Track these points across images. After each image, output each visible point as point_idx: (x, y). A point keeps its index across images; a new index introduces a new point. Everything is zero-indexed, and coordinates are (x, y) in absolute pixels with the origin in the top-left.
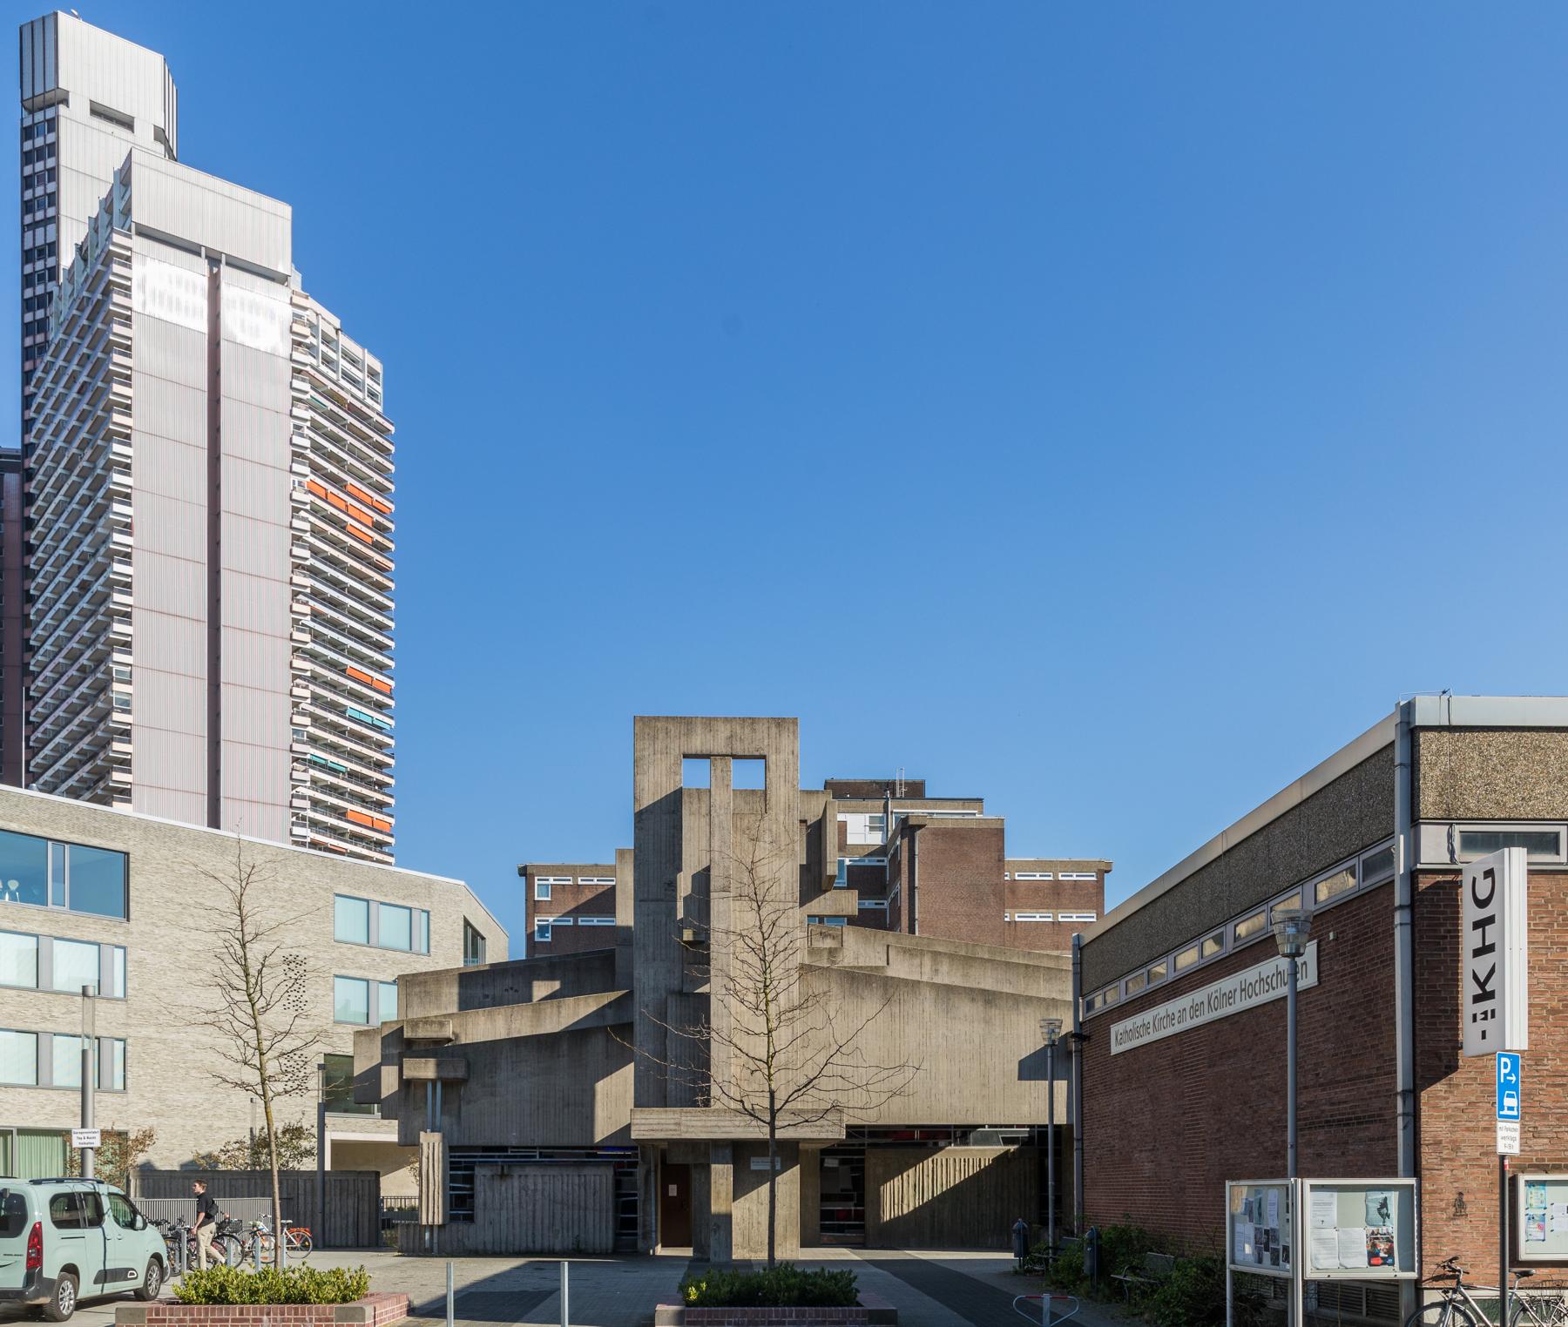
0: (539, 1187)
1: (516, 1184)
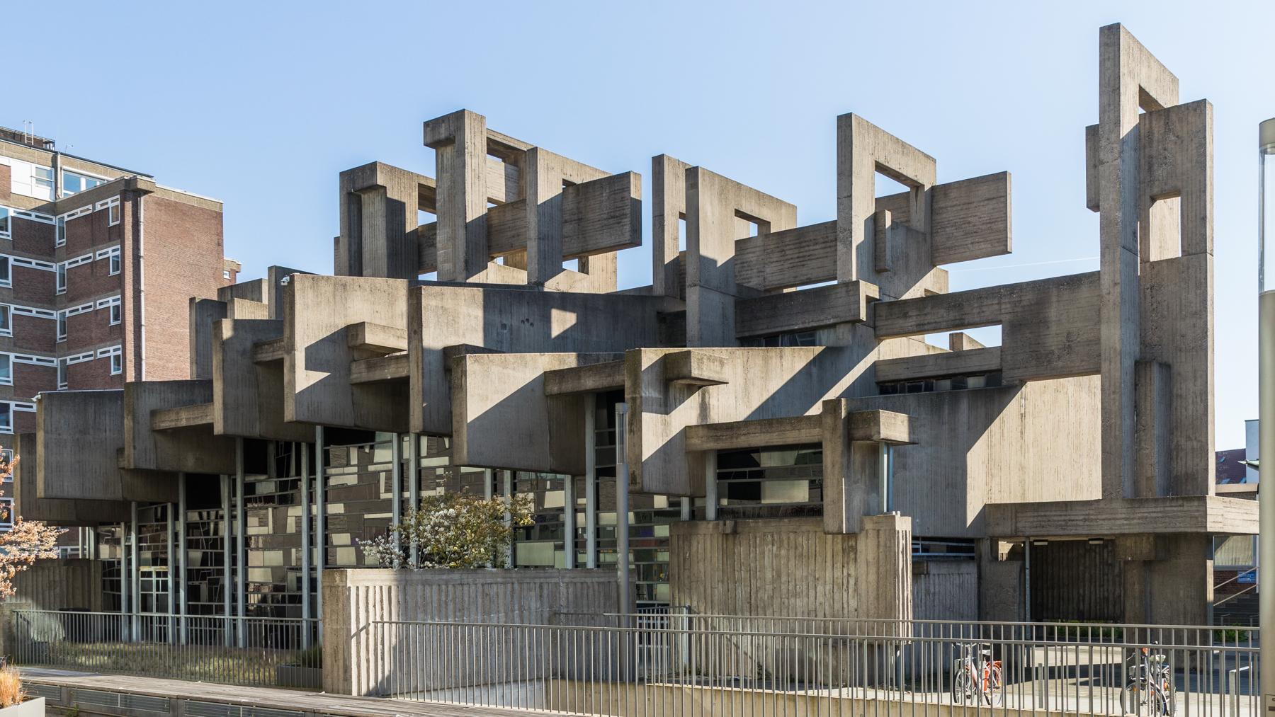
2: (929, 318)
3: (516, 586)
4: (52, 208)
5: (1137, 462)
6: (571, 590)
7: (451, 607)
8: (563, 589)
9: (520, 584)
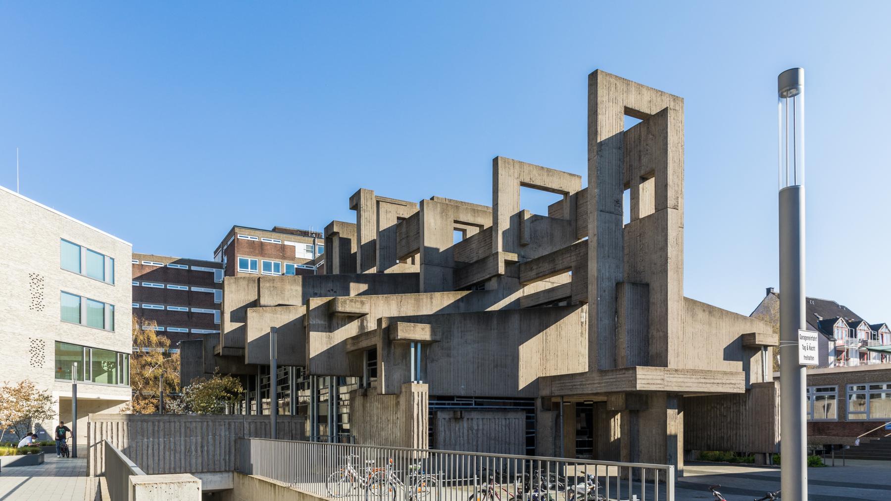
0: (481, 427)
1: (465, 425)
2: (541, 270)
3: (210, 423)
4: (313, 262)
5: (614, 347)
6: (252, 426)
7: (162, 433)
8: (246, 425)
9: (214, 422)
